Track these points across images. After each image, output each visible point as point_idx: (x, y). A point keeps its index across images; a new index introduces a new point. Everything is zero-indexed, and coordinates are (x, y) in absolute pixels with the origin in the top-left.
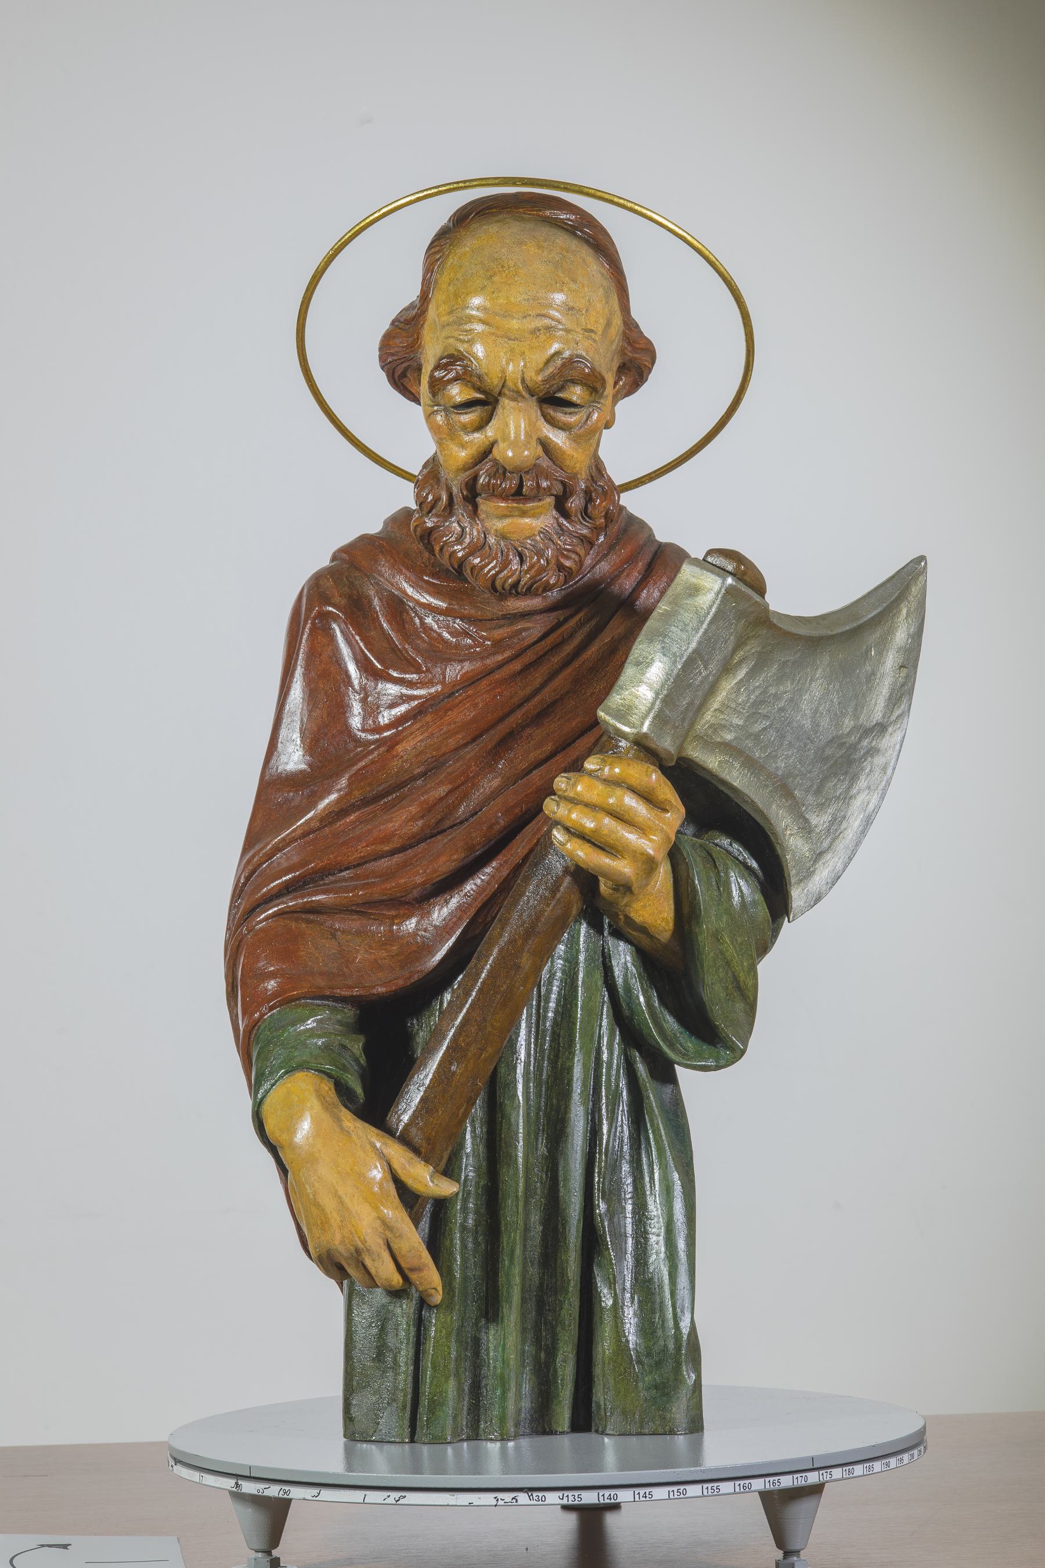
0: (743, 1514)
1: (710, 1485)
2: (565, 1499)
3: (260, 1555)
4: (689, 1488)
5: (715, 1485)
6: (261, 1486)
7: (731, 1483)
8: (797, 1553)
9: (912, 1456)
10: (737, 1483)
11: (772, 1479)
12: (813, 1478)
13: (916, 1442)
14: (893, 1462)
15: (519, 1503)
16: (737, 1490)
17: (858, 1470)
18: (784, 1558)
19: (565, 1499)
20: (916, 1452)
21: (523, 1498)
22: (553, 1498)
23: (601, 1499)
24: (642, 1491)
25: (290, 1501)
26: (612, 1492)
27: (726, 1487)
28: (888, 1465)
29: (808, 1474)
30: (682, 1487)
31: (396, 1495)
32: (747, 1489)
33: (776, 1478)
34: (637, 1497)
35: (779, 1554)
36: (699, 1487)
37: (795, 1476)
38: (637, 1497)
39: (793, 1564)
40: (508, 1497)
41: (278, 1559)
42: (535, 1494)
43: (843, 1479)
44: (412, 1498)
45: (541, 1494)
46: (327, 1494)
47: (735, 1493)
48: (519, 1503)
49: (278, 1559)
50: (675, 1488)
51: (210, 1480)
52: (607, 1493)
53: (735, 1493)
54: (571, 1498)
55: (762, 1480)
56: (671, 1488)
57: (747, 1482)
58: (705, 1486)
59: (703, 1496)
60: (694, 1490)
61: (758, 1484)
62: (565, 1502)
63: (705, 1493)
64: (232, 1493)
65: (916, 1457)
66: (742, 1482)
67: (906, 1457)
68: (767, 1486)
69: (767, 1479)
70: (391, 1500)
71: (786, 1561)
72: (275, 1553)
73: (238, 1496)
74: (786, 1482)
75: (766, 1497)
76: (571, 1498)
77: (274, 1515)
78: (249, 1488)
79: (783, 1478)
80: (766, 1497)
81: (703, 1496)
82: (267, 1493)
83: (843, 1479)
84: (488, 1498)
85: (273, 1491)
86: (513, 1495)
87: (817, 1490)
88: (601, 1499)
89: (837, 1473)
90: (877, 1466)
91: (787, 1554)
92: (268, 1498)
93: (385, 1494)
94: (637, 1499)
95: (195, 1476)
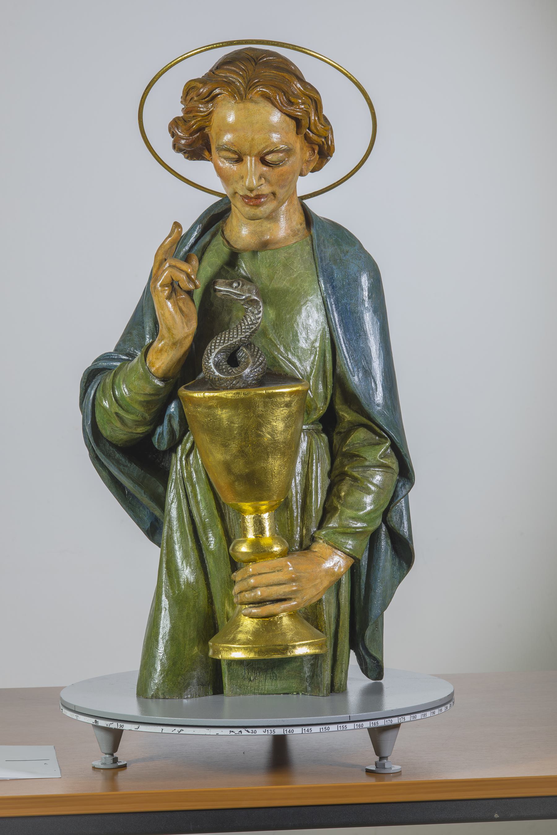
1: (341, 725)
2: (267, 732)
3: (107, 756)
5: (344, 725)
6: (108, 723)
9: (447, 708)
10: (356, 724)
11: (374, 722)
12: (395, 721)
13: (449, 700)
14: (437, 711)
15: (243, 734)
16: (356, 727)
17: (419, 716)
18: (380, 760)
19: (267, 732)
20: (448, 705)
21: (244, 732)
22: (260, 731)
23: (285, 732)
24: (306, 728)
25: (122, 731)
26: (291, 729)
27: (350, 726)
28: (434, 713)
29: (393, 719)
30: (327, 726)
31: (178, 729)
32: (361, 727)
33: (376, 721)
34: (304, 731)
35: (377, 758)
37: (386, 720)
38: (304, 731)
39: (384, 765)
40: (237, 731)
42: (250, 730)
43: (410, 721)
44: (187, 731)
45: (254, 730)
46: (143, 728)
47: (355, 729)
48: (243, 734)
50: (324, 727)
51: (82, 718)
52: (288, 729)
54: (270, 732)
55: (368, 722)
56: (321, 727)
57: (361, 723)
58: (339, 725)
59: (338, 731)
60: (333, 728)
61: (367, 724)
62: (266, 733)
63: (339, 729)
64: (93, 725)
65: (448, 708)
66: (358, 724)
67: (443, 708)
68: (371, 725)
69: (371, 722)
70: (176, 732)
73: (96, 726)
74: (381, 723)
75: (370, 730)
76: (270, 732)
77: (116, 736)
78: (102, 723)
80: (370, 730)
81: (338, 731)
82: (111, 726)
84: (226, 731)
85: (114, 725)
86: (239, 730)
88: (285, 732)
89: (407, 718)
90: (428, 714)
91: (381, 758)
92: (112, 728)
93: (174, 728)
94: (304, 732)
95: (73, 716)
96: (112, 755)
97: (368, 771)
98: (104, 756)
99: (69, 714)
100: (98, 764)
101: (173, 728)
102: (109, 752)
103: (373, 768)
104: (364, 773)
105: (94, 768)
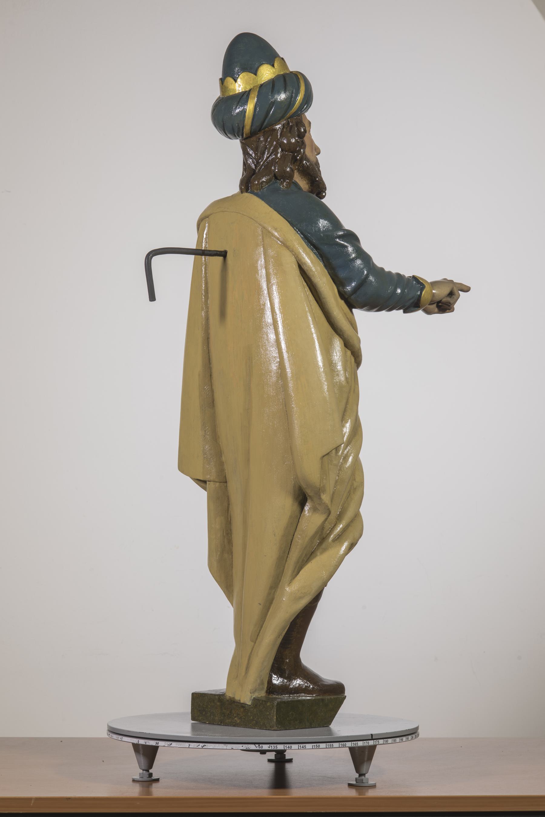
0: (341, 757)
3: (145, 772)
4: (320, 744)
7: (338, 743)
8: (364, 775)
9: (413, 737)
12: (371, 743)
14: (404, 738)
17: (390, 741)
28: (402, 740)
32: (344, 746)
35: (357, 775)
36: (325, 744)
41: (152, 774)
49: (152, 774)
51: (125, 739)
53: (339, 747)
60: (323, 745)
64: (133, 744)
67: (410, 737)
71: (361, 778)
72: (151, 771)
73: (136, 747)
74: (360, 744)
78: (142, 742)
79: (359, 742)
83: (383, 744)
87: (373, 748)
89: (381, 741)
90: (398, 740)
91: (360, 775)
96: (148, 771)
97: (350, 785)
98: (141, 771)
99: (115, 736)
100: (137, 777)
101: (199, 744)
102: (146, 768)
103: (354, 783)
104: (347, 786)
105: (134, 781)
